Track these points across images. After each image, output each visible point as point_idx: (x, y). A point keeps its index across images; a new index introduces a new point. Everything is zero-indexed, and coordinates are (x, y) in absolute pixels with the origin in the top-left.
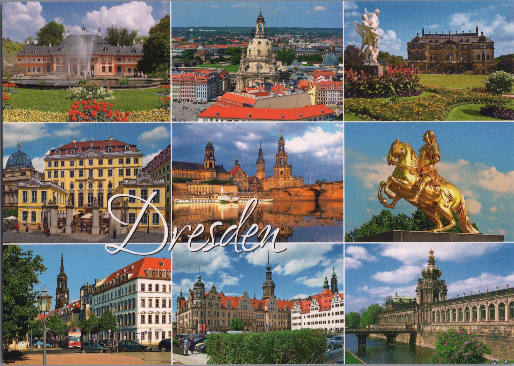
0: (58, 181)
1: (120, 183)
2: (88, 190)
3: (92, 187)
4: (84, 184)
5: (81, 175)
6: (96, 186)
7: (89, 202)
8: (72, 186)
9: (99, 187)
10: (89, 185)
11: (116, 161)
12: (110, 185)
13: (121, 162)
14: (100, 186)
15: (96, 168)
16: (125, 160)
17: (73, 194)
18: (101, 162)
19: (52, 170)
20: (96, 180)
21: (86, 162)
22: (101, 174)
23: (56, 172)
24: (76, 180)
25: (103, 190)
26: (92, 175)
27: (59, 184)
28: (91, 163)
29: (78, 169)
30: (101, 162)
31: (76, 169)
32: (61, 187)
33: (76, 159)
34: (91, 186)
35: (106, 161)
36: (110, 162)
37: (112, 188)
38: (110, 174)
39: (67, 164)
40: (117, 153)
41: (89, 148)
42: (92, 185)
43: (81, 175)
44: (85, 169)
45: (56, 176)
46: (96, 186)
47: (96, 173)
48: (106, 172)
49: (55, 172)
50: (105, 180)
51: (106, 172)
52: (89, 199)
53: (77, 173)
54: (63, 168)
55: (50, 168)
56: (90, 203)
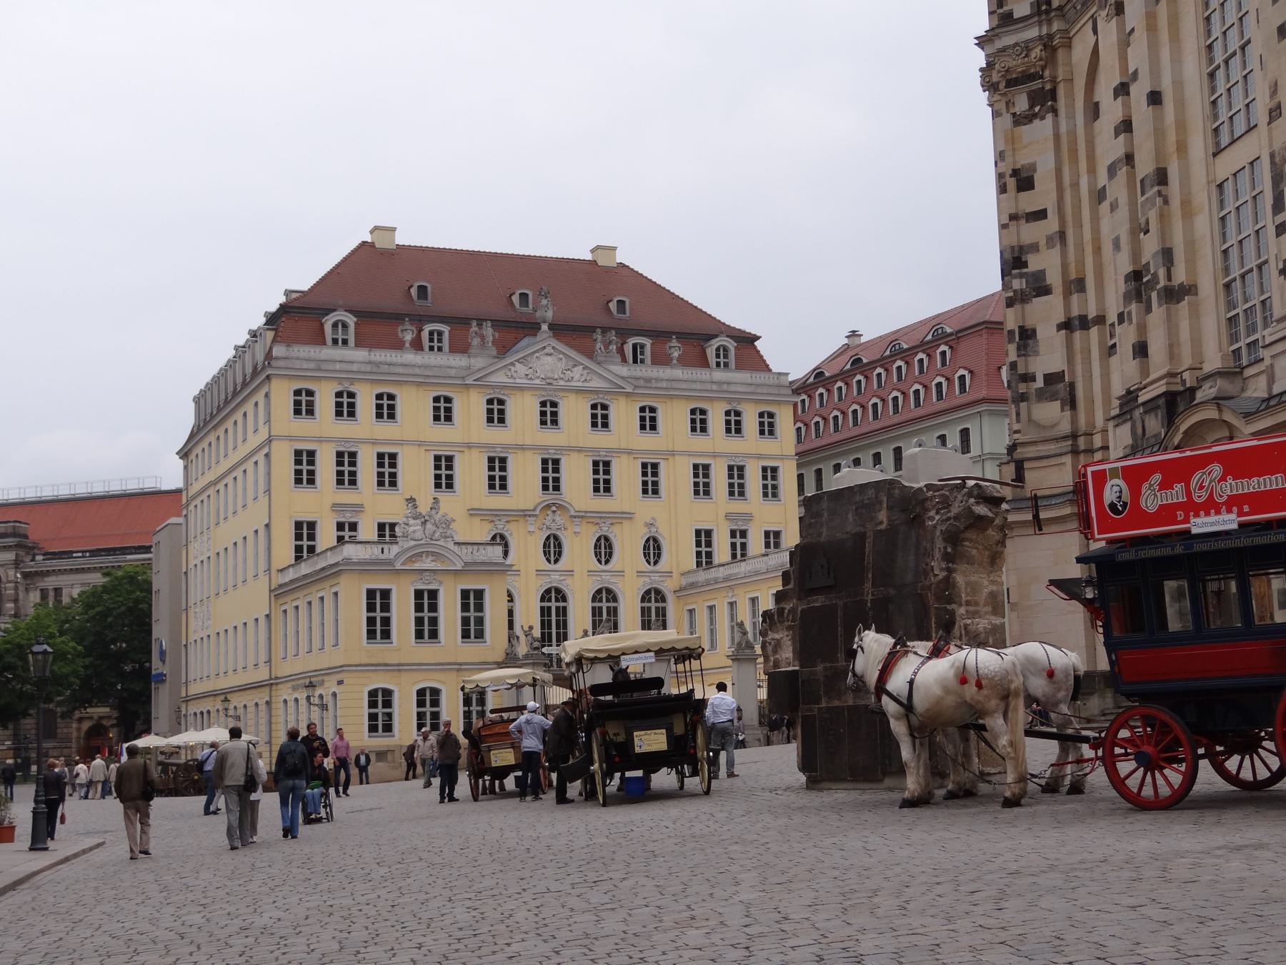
1: (704, 537)
5: (498, 483)
6: (578, 548)
10: (546, 545)
11: (674, 418)
12: (653, 549)
13: (699, 423)
14: (604, 549)
15: (580, 450)
16: (716, 420)
18: (600, 419)
19: (320, 440)
20: (582, 516)
21: (523, 410)
22: (602, 486)
26: (557, 488)
28: (549, 415)
34: (553, 548)
35: (624, 415)
36: (648, 422)
37: (664, 564)
38: (651, 488)
40: (678, 373)
41: (531, 328)
42: (559, 545)
43: (498, 483)
46: (578, 548)
47: (577, 476)
48: (626, 476)
50: (626, 516)
51: (626, 476)
53: (470, 472)
54: (385, 430)
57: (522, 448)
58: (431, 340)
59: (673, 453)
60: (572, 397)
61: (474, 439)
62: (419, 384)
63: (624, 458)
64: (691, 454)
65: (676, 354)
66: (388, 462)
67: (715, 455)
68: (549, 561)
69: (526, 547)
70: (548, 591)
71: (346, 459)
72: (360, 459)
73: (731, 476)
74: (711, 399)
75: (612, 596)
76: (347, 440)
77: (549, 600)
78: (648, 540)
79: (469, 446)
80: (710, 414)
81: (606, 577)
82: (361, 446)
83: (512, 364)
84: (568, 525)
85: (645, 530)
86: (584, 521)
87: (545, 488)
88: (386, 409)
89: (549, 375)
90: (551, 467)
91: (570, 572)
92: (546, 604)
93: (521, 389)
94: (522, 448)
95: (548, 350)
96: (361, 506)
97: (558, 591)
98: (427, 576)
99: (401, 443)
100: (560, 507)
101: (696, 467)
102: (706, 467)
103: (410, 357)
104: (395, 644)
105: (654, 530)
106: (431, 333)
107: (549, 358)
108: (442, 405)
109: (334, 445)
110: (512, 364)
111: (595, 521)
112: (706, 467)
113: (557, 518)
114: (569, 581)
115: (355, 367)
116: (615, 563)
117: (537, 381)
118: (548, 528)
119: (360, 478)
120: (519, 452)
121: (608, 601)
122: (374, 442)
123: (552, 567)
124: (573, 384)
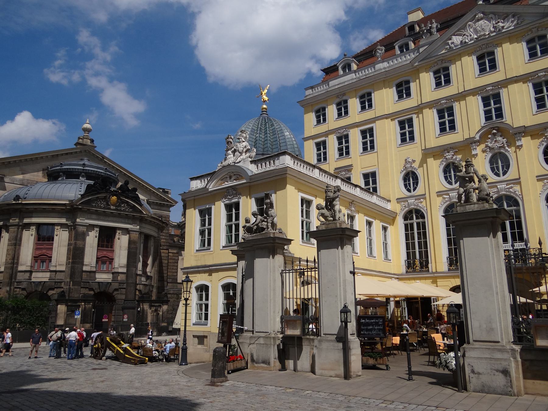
0: (349, 168)
3: (507, 166)
8: (410, 178)
17: (420, 214)
20: (524, 131)
23: (343, 139)
24: (429, 153)
27: (358, 178)
29: (430, 105)
31: (419, 109)
32: (367, 190)
33: (415, 71)
34: (500, 163)
39: (386, 99)
44: (461, 96)
45: (344, 151)
49: (339, 139)
54: (369, 114)
55: (323, 128)
58: (402, 51)
66: (368, 134)
68: (498, 175)
71: (343, 139)
87: (488, 118)
88: (366, 102)
89: (482, 33)
90: (492, 100)
91: (517, 181)
96: (351, 166)
100: (499, 129)
106: (401, 48)
107: (481, 22)
114: (517, 188)
115: (346, 84)
117: (473, 42)
123: (502, 178)
124: (504, 31)
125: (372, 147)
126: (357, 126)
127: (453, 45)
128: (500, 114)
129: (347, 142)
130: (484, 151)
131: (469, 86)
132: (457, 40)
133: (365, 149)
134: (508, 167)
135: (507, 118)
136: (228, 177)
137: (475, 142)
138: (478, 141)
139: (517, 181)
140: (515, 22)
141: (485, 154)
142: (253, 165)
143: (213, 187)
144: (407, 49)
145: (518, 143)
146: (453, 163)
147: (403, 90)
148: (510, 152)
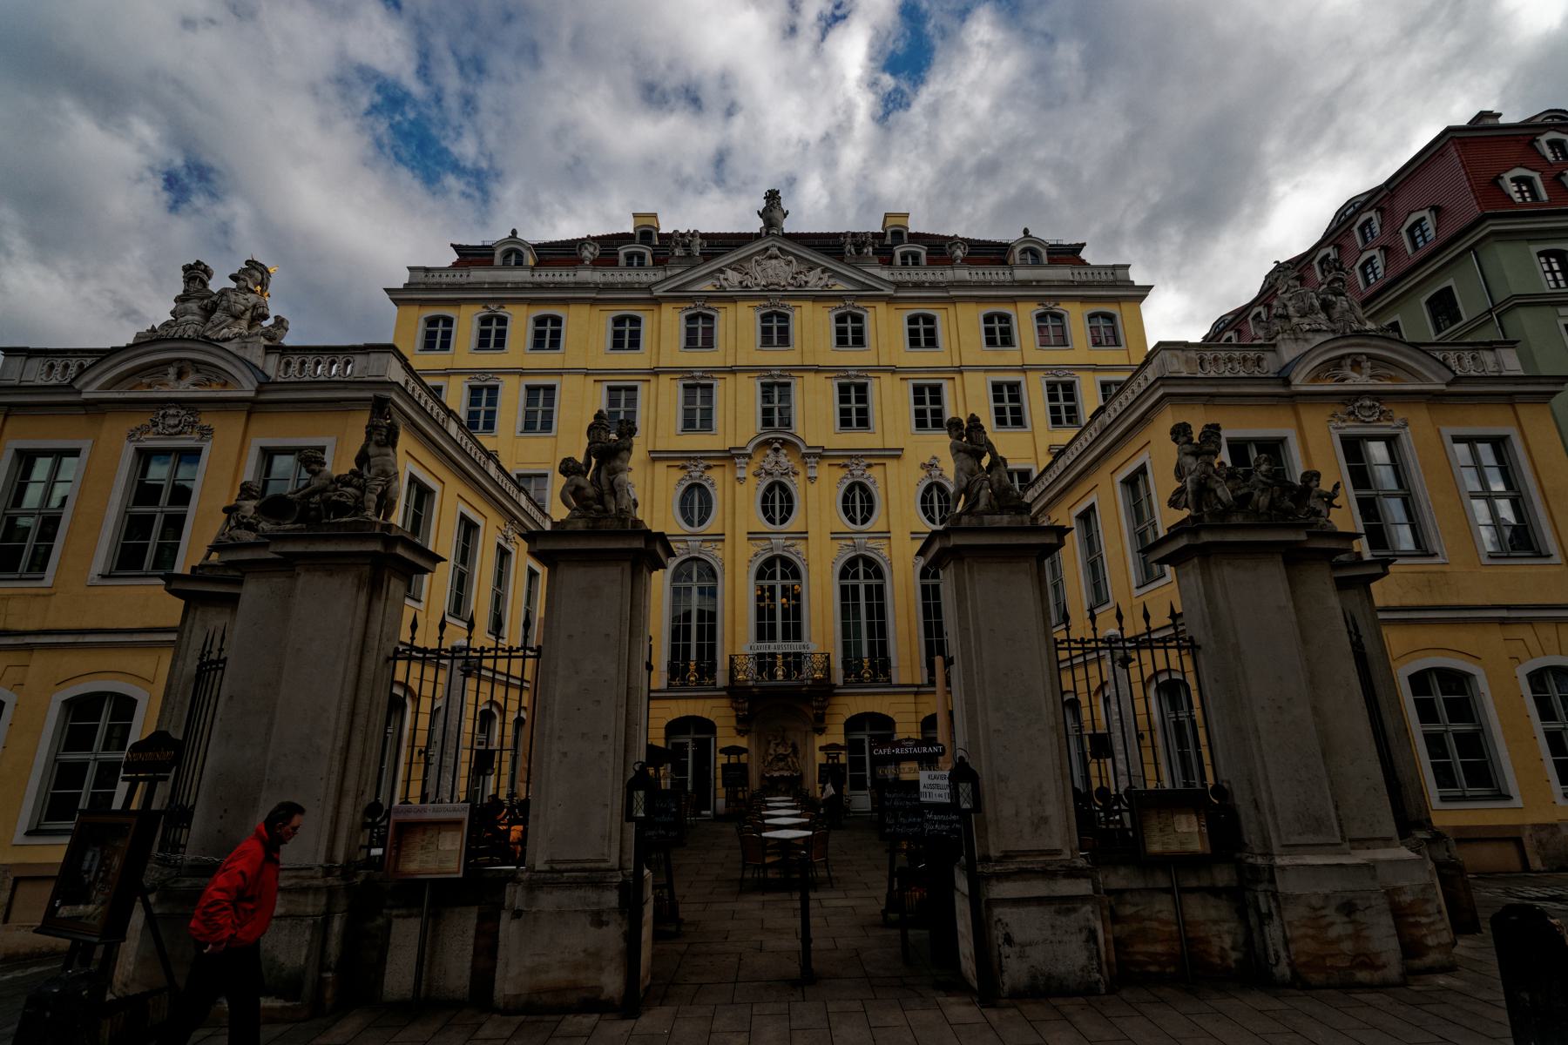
2: (753, 536)
4: (718, 480)
5: (697, 417)
7: (764, 632)
9: (848, 510)
13: (999, 333)
14: (859, 502)
15: (817, 370)
19: (447, 373)
20: (821, 454)
23: (484, 394)
25: (886, 535)
28: (776, 331)
30: (850, 333)
34: (777, 502)
40: (963, 274)
42: (788, 499)
43: (697, 417)
50: (896, 454)
52: (764, 614)
54: (547, 359)
56: (779, 646)
57: (733, 371)
59: (960, 370)
60: (807, 306)
61: (665, 362)
62: (594, 302)
63: (886, 377)
64: (988, 369)
65: (959, 253)
67: (1023, 369)
68: (771, 521)
69: (737, 502)
70: (770, 563)
72: (502, 397)
73: (1053, 397)
74: (1013, 300)
75: (874, 569)
76: (484, 372)
77: (773, 576)
78: (928, 489)
79: (656, 372)
80: (1014, 319)
81: (860, 540)
82: (502, 378)
83: (721, 271)
84: (799, 469)
85: (924, 473)
86: (825, 463)
87: (767, 422)
88: (547, 335)
90: (776, 391)
91: (803, 535)
92: (766, 583)
93: (733, 300)
94: (733, 371)
95: (775, 251)
97: (786, 562)
98: (173, 417)
99: (559, 372)
100: (785, 443)
101: (997, 387)
102: (1014, 387)
103: (585, 275)
104: (48, 581)
105: (936, 473)
107: (774, 262)
108: (627, 328)
109: (465, 378)
110: (721, 271)
111: (846, 461)
112: (1014, 387)
113: (783, 459)
114: (800, 546)
116: (877, 523)
118: (769, 474)
119: (499, 420)
120: (730, 378)
121: (867, 576)
122: (521, 372)
123: (777, 528)
125: (547, 426)
126: (521, 374)
127: (725, 284)
128: (787, 423)
129: (492, 401)
130: (757, 475)
131: (742, 361)
132: (733, 277)
133: (529, 426)
134: (790, 510)
135: (798, 427)
136: (172, 371)
137: (744, 456)
138: (749, 456)
139: (803, 535)
140: (822, 283)
141: (757, 480)
142: (273, 360)
143: (107, 386)
144: (641, 264)
145: (812, 473)
146: (700, 486)
147: (626, 335)
148: (796, 485)
